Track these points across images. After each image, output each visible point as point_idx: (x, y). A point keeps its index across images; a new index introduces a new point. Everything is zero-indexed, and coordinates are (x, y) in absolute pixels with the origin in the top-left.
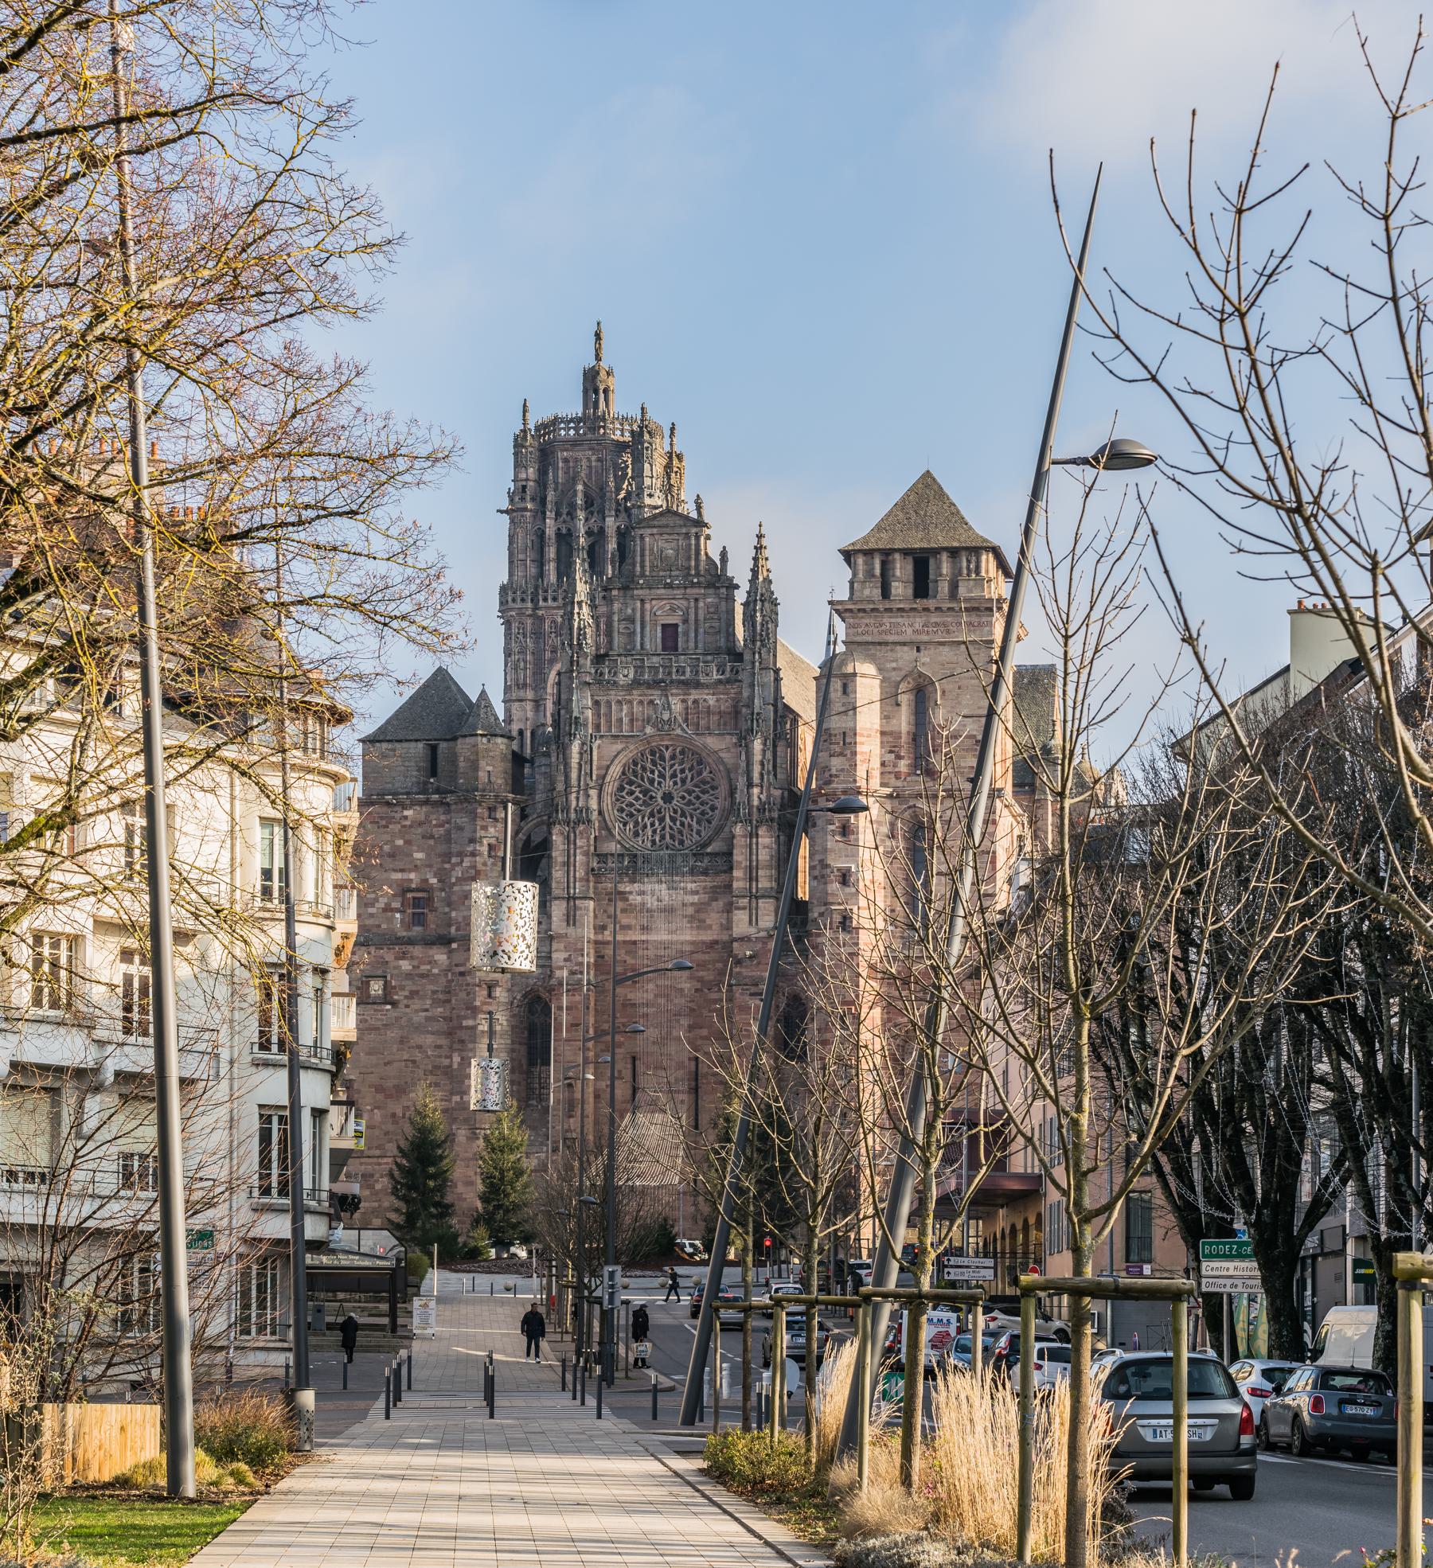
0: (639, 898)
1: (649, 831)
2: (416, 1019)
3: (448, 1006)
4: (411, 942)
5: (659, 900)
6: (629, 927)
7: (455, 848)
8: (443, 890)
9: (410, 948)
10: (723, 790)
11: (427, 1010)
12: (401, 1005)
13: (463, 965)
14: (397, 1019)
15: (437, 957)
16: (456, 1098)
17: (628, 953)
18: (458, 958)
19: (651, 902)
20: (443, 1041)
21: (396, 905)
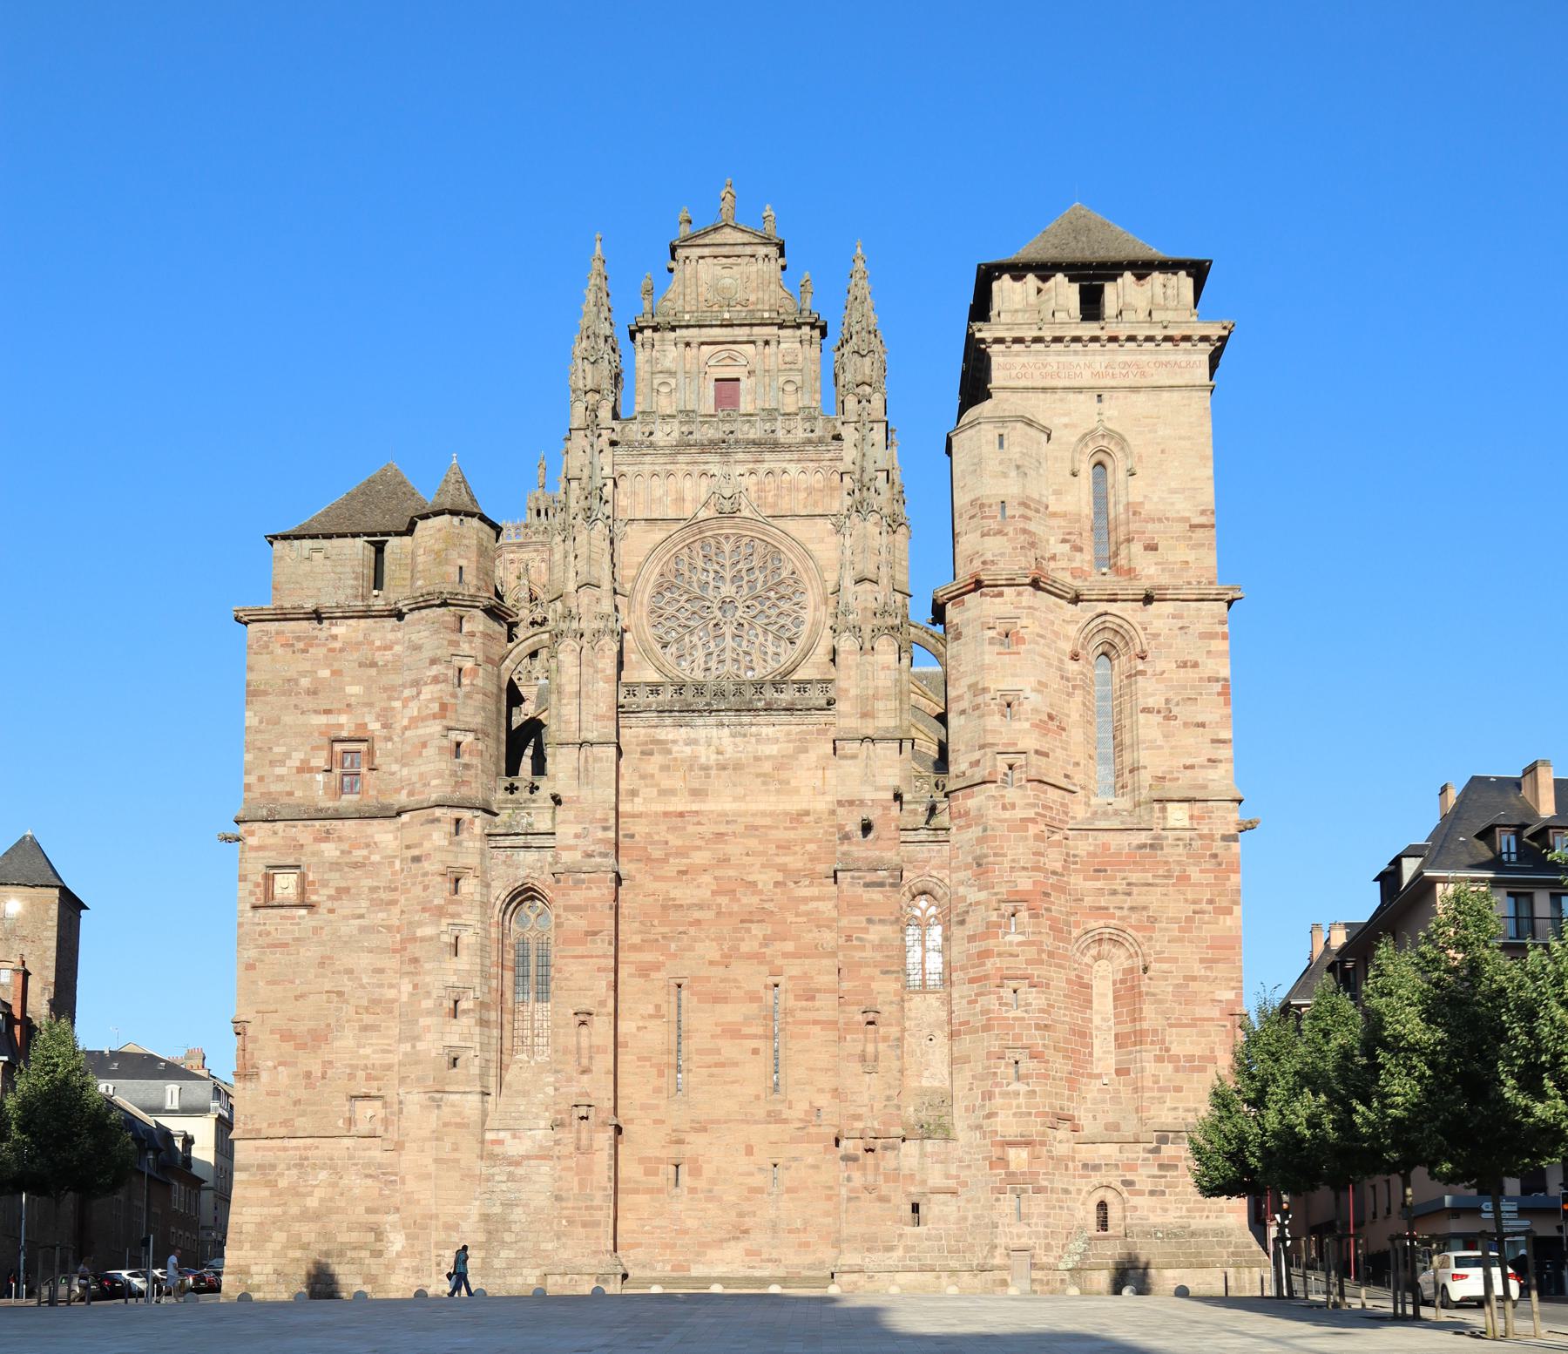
0: (688, 750)
1: (700, 654)
2: (344, 930)
3: (396, 910)
5: (719, 753)
6: (672, 792)
7: (408, 676)
8: (389, 739)
11: (361, 916)
12: (322, 910)
13: (421, 844)
14: (315, 930)
15: (378, 838)
16: (407, 1047)
18: (413, 835)
19: (706, 756)
20: (390, 963)
21: (320, 761)
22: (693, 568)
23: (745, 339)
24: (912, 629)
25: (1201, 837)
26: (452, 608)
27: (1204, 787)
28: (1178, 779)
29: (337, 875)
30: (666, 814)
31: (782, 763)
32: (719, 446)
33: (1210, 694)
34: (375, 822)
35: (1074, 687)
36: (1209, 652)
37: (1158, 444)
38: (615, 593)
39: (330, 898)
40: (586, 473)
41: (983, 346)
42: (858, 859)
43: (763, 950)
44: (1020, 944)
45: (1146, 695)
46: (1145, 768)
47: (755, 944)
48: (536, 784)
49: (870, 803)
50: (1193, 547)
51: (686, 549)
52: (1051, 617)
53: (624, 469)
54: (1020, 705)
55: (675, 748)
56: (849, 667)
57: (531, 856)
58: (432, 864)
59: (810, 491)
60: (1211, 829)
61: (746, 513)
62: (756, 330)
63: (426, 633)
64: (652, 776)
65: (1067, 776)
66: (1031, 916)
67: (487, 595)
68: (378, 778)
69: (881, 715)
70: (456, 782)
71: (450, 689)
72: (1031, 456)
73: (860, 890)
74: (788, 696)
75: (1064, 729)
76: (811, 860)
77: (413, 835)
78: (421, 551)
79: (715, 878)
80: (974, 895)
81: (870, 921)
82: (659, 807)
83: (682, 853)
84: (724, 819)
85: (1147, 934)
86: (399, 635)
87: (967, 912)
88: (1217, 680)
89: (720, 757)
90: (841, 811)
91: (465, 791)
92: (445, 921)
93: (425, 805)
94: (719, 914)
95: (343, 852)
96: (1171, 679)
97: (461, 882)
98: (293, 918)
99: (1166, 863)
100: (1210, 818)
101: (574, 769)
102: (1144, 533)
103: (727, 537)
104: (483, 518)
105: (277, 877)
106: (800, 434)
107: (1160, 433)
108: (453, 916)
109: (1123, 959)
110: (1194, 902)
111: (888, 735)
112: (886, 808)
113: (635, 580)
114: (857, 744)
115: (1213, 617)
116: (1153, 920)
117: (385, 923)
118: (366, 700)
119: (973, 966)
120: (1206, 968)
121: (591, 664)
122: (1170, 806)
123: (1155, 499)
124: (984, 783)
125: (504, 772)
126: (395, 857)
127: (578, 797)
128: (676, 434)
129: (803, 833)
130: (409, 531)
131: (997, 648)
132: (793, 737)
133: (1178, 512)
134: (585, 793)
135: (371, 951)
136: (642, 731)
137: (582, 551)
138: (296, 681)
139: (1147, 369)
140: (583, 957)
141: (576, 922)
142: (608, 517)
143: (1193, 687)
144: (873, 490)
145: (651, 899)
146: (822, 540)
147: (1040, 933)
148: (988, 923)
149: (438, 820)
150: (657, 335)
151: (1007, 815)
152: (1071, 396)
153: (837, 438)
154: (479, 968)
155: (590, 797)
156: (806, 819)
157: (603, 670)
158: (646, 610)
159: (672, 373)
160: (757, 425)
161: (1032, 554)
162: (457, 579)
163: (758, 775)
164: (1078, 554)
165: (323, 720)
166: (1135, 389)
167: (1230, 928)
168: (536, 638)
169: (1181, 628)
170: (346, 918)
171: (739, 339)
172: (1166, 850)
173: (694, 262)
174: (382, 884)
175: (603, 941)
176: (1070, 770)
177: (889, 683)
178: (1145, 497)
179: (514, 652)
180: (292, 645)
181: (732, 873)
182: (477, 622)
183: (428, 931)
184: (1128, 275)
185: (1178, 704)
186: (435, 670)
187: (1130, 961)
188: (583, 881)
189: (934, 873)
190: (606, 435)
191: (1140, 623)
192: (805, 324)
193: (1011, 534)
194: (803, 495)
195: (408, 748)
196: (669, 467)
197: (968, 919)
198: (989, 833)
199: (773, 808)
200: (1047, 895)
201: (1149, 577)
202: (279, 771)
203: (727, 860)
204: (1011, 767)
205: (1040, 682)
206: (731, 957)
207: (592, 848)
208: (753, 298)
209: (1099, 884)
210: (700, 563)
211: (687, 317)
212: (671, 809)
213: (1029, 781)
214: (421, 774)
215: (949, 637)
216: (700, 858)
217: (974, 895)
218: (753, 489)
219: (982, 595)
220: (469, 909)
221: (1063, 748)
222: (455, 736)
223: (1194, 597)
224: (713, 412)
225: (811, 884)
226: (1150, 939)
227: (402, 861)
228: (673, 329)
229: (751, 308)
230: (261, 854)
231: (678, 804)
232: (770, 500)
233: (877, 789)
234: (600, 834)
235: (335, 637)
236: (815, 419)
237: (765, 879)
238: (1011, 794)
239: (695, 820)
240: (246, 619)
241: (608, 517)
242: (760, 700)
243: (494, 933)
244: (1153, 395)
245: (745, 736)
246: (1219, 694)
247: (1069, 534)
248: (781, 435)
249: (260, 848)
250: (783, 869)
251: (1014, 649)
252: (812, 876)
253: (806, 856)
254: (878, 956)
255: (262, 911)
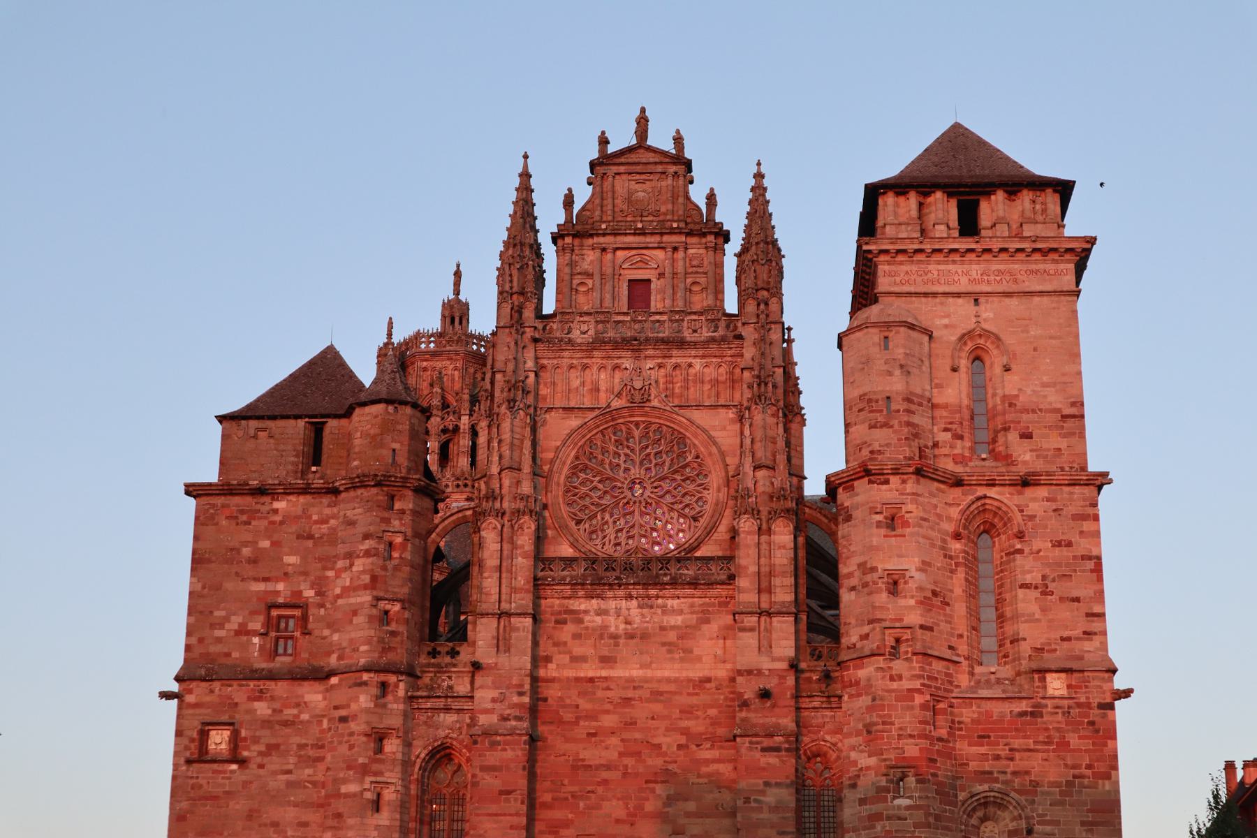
0: (598, 619)
3: (321, 767)
4: (272, 676)
7: (341, 549)
8: (322, 606)
9: (271, 685)
10: (715, 478)
11: (289, 772)
12: (253, 766)
13: (348, 706)
14: (246, 784)
15: (308, 698)
17: (582, 694)
18: (340, 697)
19: (616, 625)
20: (312, 816)
21: (257, 625)
22: (604, 451)
23: (656, 245)
24: (807, 510)
25: (1079, 705)
26: (385, 489)
27: (1081, 658)
28: (1055, 650)
29: (266, 732)
30: (578, 679)
31: (686, 633)
32: (633, 345)
33: (1083, 571)
34: (306, 683)
35: (957, 564)
36: (1081, 532)
37: (1031, 343)
38: (534, 474)
39: (261, 754)
40: (511, 366)
41: (870, 256)
42: (755, 725)
43: (666, 810)
44: (908, 808)
45: (1024, 573)
46: (1025, 639)
47: (660, 804)
48: (458, 649)
49: (767, 673)
50: (1065, 436)
51: (600, 435)
52: (934, 501)
53: (545, 362)
54: (906, 583)
55: (587, 618)
56: (748, 546)
57: (450, 718)
58: (358, 725)
59: (715, 382)
60: (1088, 698)
61: (655, 403)
62: (666, 238)
63: (360, 511)
64: (565, 644)
65: (951, 648)
66: (918, 782)
67: (417, 476)
68: (310, 642)
69: (778, 590)
70: (383, 648)
71: (381, 562)
72: (914, 356)
73: (758, 755)
74: (689, 572)
75: (948, 604)
76: (712, 724)
77: (340, 697)
78: (358, 434)
79: (622, 740)
80: (865, 761)
81: (767, 784)
82: (571, 673)
83: (592, 716)
84: (632, 684)
85: (1030, 798)
86: (335, 510)
87: (858, 776)
88: (1090, 558)
89: (629, 627)
90: (739, 679)
91: (391, 656)
92: (369, 779)
93: (354, 669)
94: (625, 774)
95: (274, 711)
96: (1047, 557)
97: (385, 742)
98: (224, 772)
99: (1047, 729)
100: (1086, 687)
101: (493, 637)
102: (1019, 422)
103: (637, 424)
104: (415, 405)
105: (213, 733)
106: (705, 334)
107: (1032, 333)
108: (376, 774)
109: (1007, 821)
110: (1074, 767)
111: (784, 610)
112: (782, 678)
113: (552, 462)
114: (755, 619)
115: (1084, 500)
116: (1035, 784)
117: (310, 779)
118: (302, 569)
119: (865, 828)
120: (1087, 831)
121: (512, 541)
122: (1049, 677)
123: (1029, 392)
124: (873, 655)
125: (427, 637)
126: (324, 716)
127: (496, 664)
128: (591, 332)
129: (704, 698)
130: (348, 414)
131: (883, 531)
132: (697, 609)
133: (1051, 403)
134: (503, 659)
135: (296, 805)
136: (557, 602)
137: (506, 436)
138: (239, 551)
139: (1019, 276)
140: (496, 815)
141: (490, 782)
142: (529, 406)
143: (1068, 565)
144: (770, 385)
145: (563, 758)
146: (724, 428)
147: (927, 797)
148: (878, 787)
149: (365, 684)
150: (577, 242)
151: (895, 685)
152: (951, 300)
153: (739, 337)
154: (398, 823)
155: (507, 664)
156: (708, 685)
157: (522, 546)
158: (562, 489)
159: (590, 275)
160: (666, 325)
161: (915, 444)
162: (390, 461)
163: (664, 644)
164: (959, 442)
165: (260, 587)
166: (1008, 294)
167: (1109, 792)
168: (460, 515)
169: (1055, 510)
170: (275, 773)
171: (651, 245)
172: (1045, 719)
173: (610, 179)
174: (310, 742)
175: (516, 800)
176: (954, 641)
177: (785, 561)
178: (1020, 390)
179: (440, 527)
180: (236, 518)
181: (638, 736)
182: (407, 503)
183: (352, 788)
184: (1000, 196)
185: (1054, 580)
186: (368, 544)
187: (1014, 823)
188: (499, 743)
189: (828, 738)
190: (529, 333)
191: (1016, 506)
192: (711, 233)
193: (896, 426)
194: (707, 387)
195: (339, 615)
196: (585, 361)
197: (859, 783)
198: (878, 702)
199: (677, 675)
200: (933, 761)
201: (1025, 463)
202: (219, 633)
203: (635, 723)
204: (898, 641)
205: (924, 562)
206: (635, 815)
207: (508, 712)
208: (663, 209)
209: (983, 750)
210: (612, 448)
211: (604, 226)
212: (582, 675)
213: (915, 654)
214: (351, 641)
215: (840, 519)
216: (609, 721)
217: (865, 761)
218: (662, 381)
219: (870, 482)
220: (391, 767)
221: (947, 622)
222: (383, 605)
223: (1067, 482)
224: (626, 311)
225: (712, 747)
226: (1033, 802)
227: (330, 720)
228: (592, 236)
229: (661, 218)
230: (198, 711)
231: (589, 671)
232: (677, 391)
233: (774, 659)
234: (515, 699)
235: (276, 511)
236: (719, 320)
237: (669, 741)
238: (898, 666)
239: (605, 685)
240: (195, 493)
241: (529, 406)
242: (665, 575)
243: (414, 790)
244: (1024, 300)
245: (652, 607)
246: (1092, 571)
247: (951, 423)
248: (687, 335)
249: (196, 705)
250: (685, 732)
251: (899, 531)
252: (714, 741)
253: (708, 721)
254: (775, 818)
255: (196, 766)
